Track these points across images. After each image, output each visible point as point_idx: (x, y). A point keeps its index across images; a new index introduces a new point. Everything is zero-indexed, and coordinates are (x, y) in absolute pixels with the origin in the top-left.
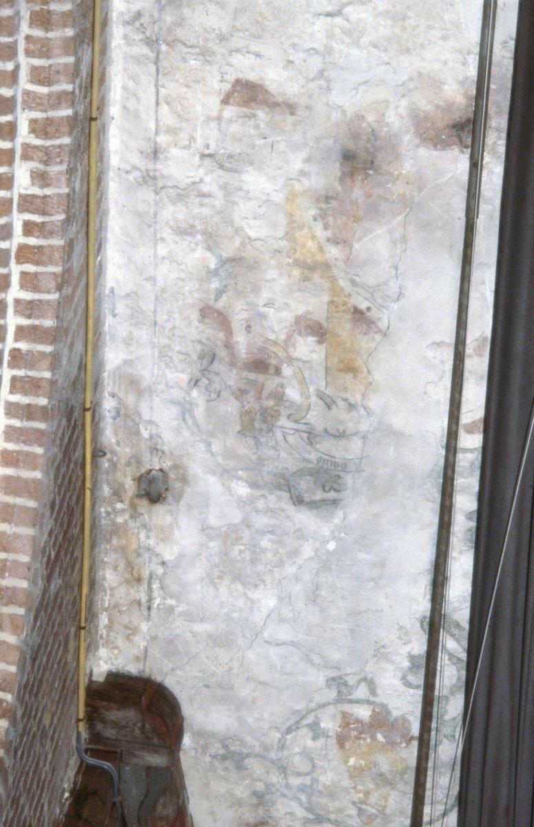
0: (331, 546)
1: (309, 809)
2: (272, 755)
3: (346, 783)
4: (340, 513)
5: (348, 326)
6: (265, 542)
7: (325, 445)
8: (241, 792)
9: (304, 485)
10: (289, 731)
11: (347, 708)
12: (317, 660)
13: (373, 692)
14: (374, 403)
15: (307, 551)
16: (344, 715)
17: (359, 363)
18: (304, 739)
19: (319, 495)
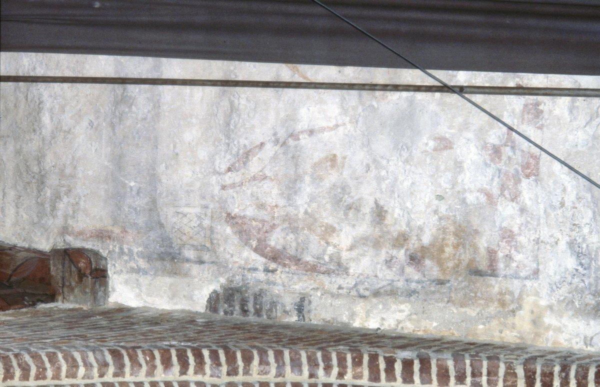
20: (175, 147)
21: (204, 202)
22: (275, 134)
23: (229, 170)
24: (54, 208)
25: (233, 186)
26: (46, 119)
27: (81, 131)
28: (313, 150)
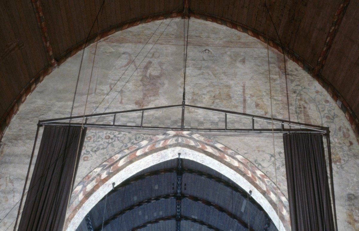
0: (347, 188)
1: (343, 149)
2: (350, 156)
3: (338, 153)
4: (347, 193)
5: (351, 222)
6: (357, 188)
7: (351, 204)
8: (353, 151)
9: (353, 197)
10: (348, 160)
11: (340, 164)
12: (346, 171)
13: (337, 167)
14: (345, 211)
15: (351, 187)
16: (341, 163)
17: (349, 216)
18: (346, 159)
19: (350, 196)
20: (17, 167)
21: (4, 173)
22: (15, 189)
23: (10, 179)
24: (10, 142)
25: (6, 180)
26: (28, 141)
27: (25, 148)
28: (10, 196)
